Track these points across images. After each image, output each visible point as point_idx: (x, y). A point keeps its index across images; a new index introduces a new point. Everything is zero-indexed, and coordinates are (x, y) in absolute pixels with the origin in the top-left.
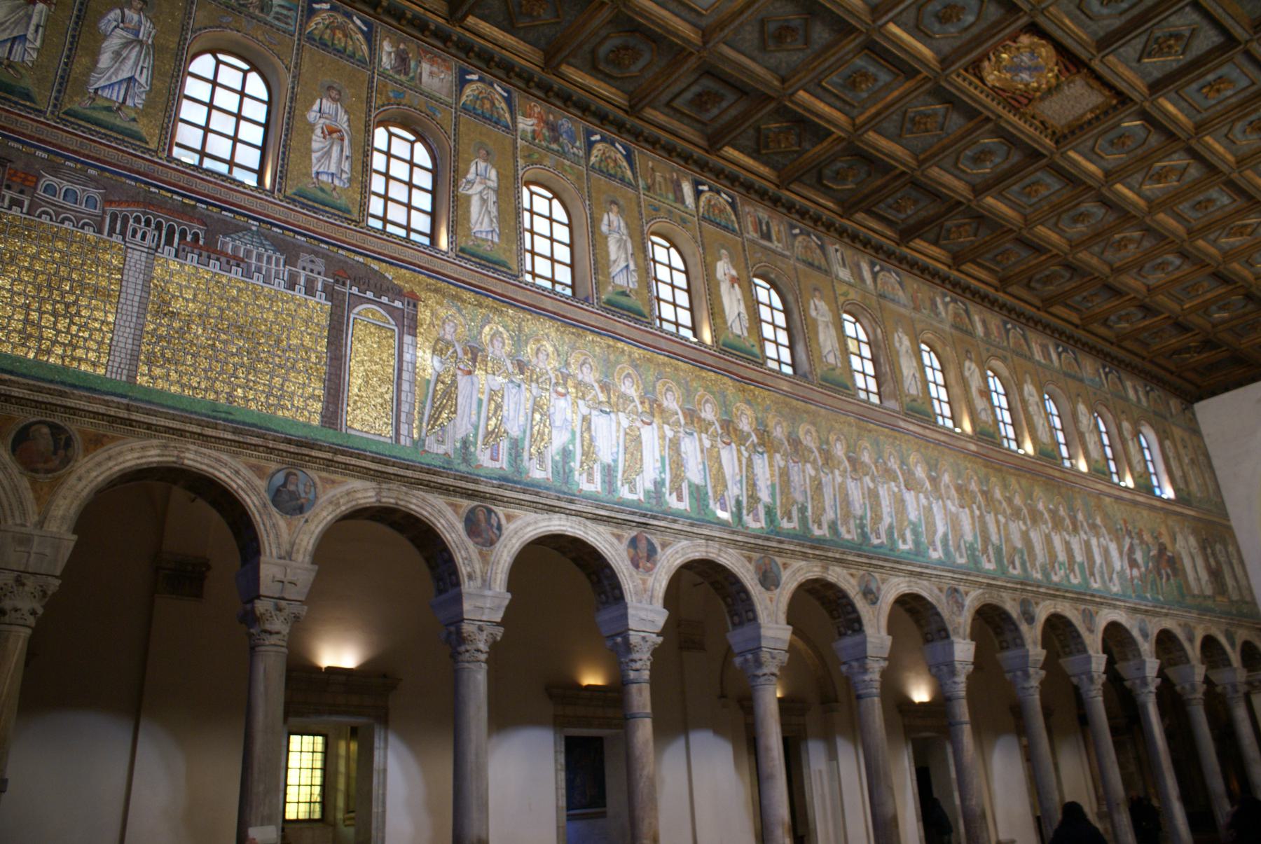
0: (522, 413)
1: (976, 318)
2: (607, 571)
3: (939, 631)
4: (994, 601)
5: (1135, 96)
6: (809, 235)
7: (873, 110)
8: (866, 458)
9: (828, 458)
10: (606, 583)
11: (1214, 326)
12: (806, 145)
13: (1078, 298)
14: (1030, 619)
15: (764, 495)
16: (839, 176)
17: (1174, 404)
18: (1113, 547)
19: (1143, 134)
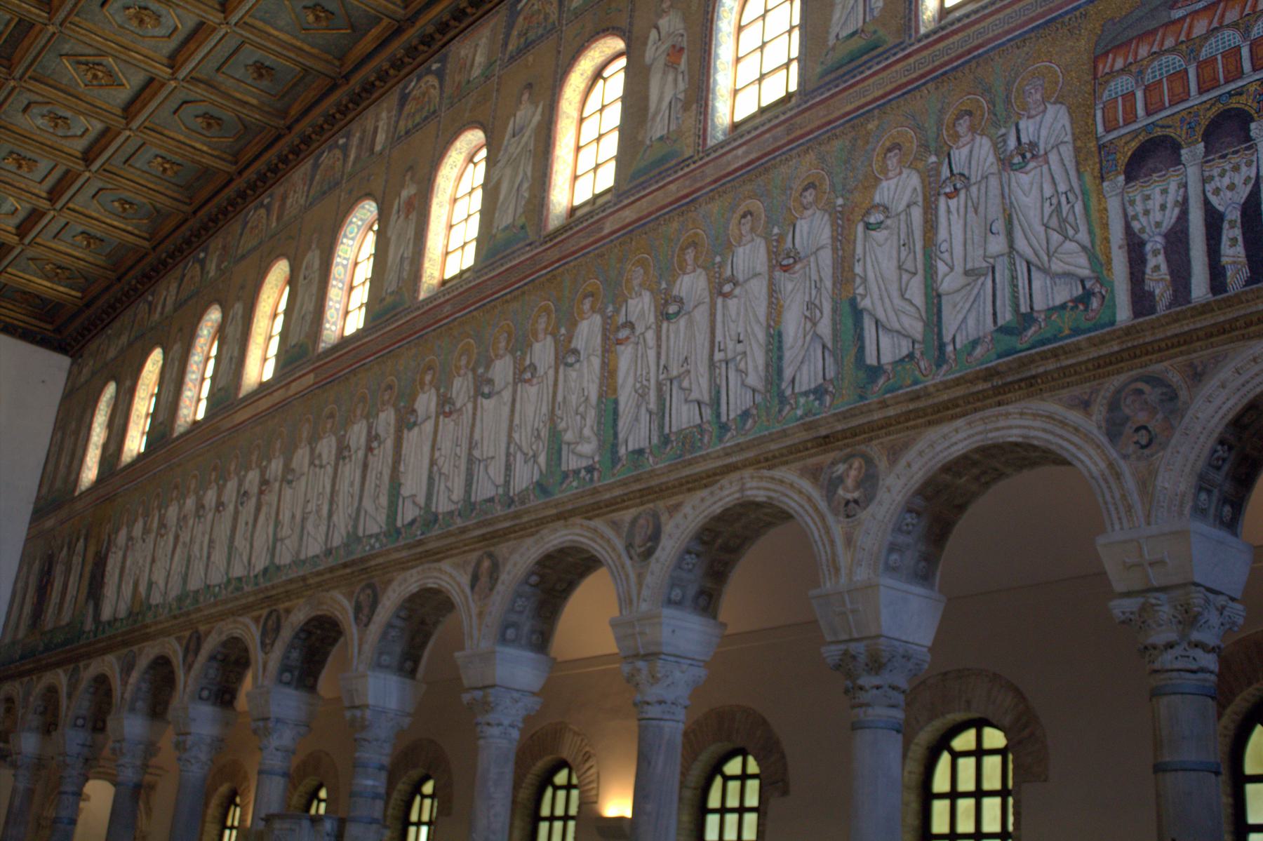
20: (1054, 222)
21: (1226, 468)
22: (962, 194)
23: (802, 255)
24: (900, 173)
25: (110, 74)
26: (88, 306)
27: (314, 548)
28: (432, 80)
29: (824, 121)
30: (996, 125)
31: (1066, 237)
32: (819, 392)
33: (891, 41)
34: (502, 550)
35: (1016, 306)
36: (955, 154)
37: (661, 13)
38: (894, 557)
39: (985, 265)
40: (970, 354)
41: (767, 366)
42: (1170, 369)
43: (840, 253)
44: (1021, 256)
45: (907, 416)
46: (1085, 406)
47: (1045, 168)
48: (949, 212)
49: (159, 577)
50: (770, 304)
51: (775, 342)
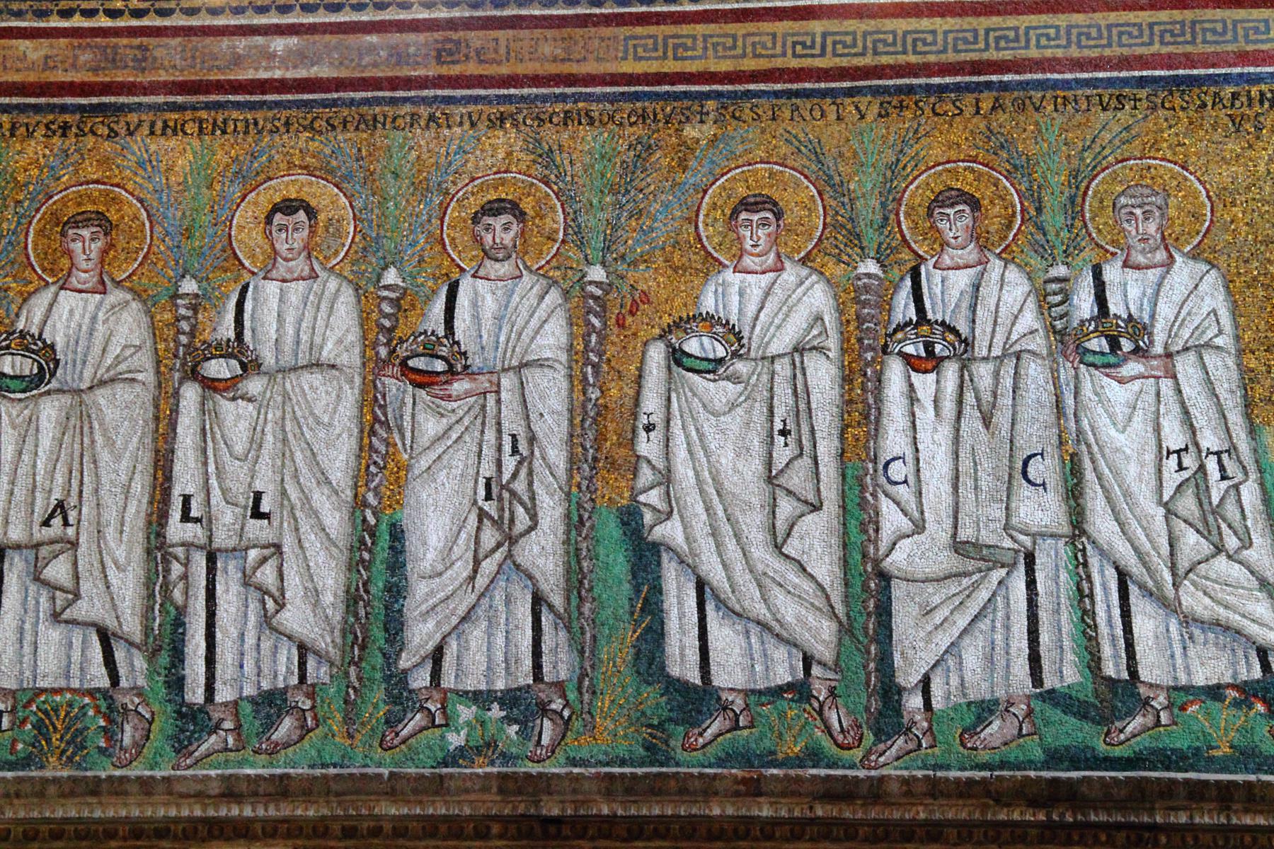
20: (1188, 504)
22: (951, 371)
23: (476, 362)
24: (779, 269)
29: (553, 69)
31: (1219, 549)
35: (1093, 662)
36: (932, 279)
39: (1008, 543)
40: (971, 731)
41: (352, 600)
43: (594, 394)
44: (1102, 553)
47: (1166, 385)
48: (912, 396)
50: (364, 448)
51: (379, 550)
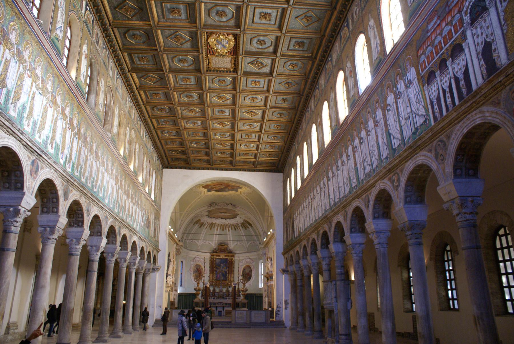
0: (14, 78)
1: (133, 111)
2: (19, 173)
3: (97, 232)
4: (114, 225)
5: (239, 72)
6: (107, 50)
7: (168, 24)
8: (100, 154)
9: (91, 149)
10: (13, 178)
11: (190, 148)
12: (134, 18)
13: (163, 120)
14: (120, 235)
15: (73, 157)
16: (134, 36)
17: (161, 166)
18: (140, 213)
19: (228, 83)
20: (417, 101)
21: (464, 161)
25: (255, 113)
26: (280, 161)
27: (320, 215)
28: (317, 90)
30: (403, 76)
32: (387, 158)
33: (383, 58)
34: (347, 209)
37: (347, 62)
38: (408, 199)
42: (443, 137)
45: (400, 162)
46: (430, 151)
49: (301, 226)
